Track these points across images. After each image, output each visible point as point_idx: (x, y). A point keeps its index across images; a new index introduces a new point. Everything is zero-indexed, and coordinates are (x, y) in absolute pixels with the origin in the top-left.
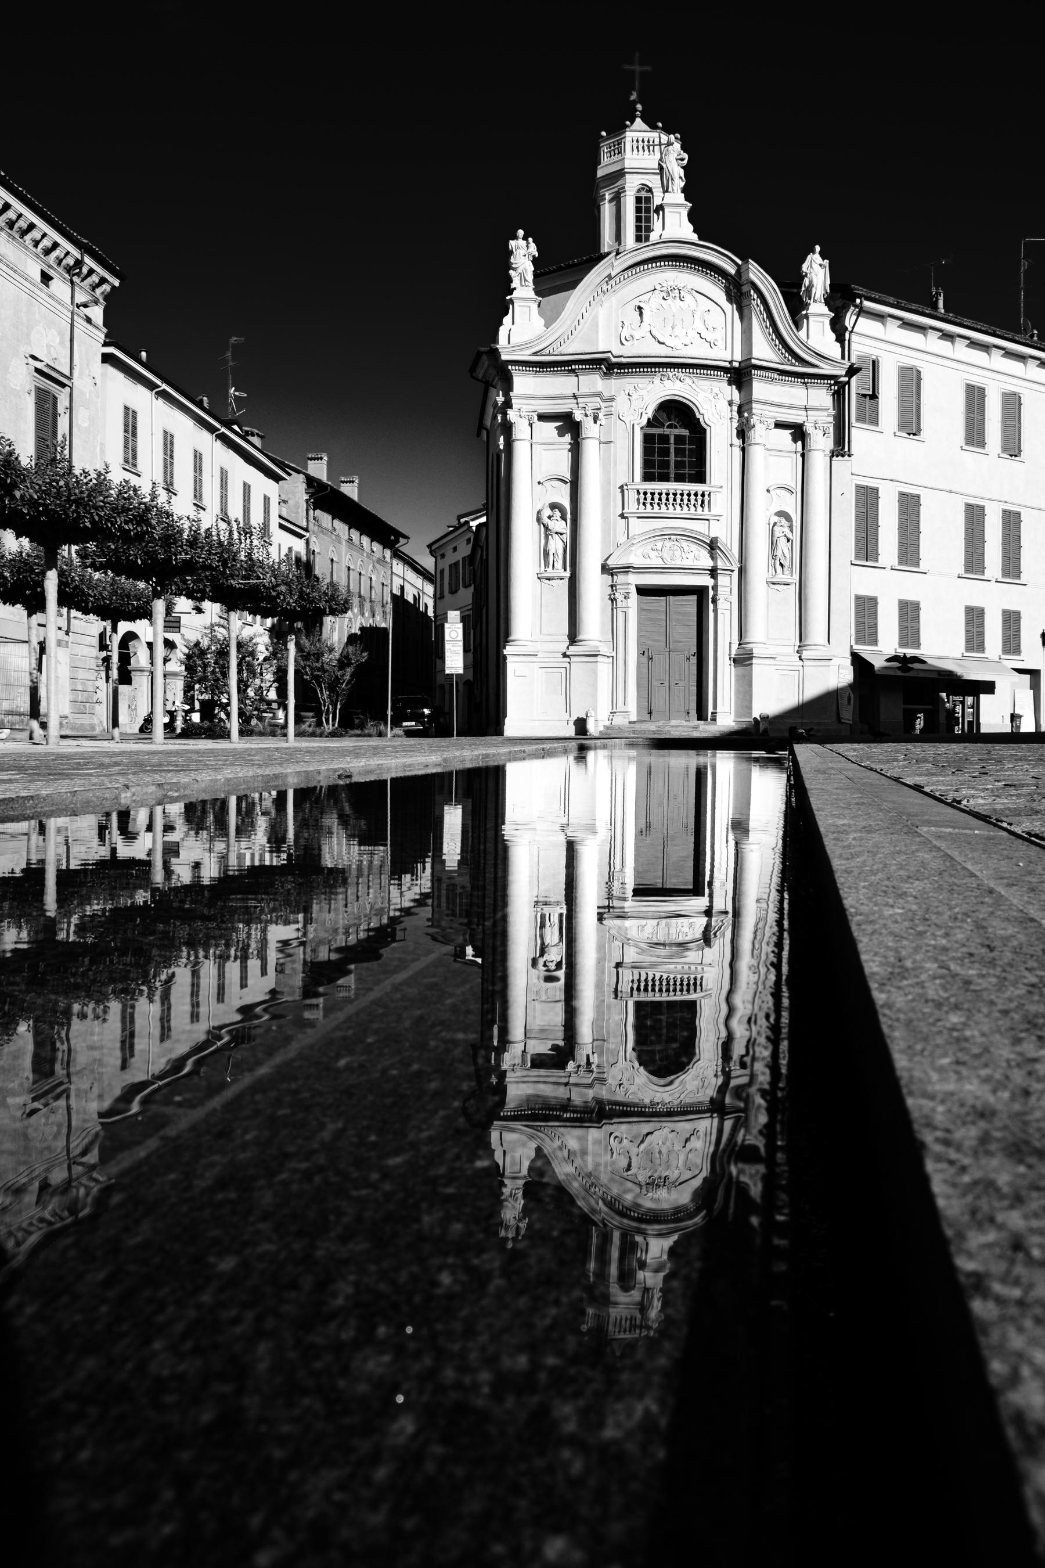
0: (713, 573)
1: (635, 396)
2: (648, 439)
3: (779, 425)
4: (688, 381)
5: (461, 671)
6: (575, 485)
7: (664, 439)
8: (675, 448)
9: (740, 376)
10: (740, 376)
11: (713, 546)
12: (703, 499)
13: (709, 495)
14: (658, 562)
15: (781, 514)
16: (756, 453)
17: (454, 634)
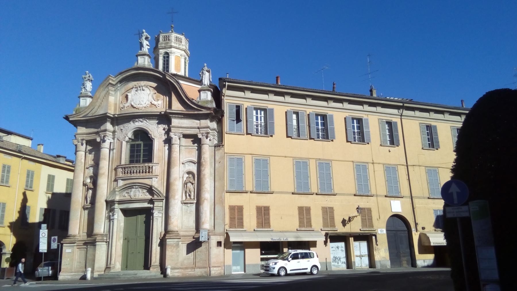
0: (151, 201)
1: (124, 129)
2: (132, 146)
3: (186, 136)
4: (145, 121)
5: (46, 251)
6: (199, 163)
7: (139, 145)
8: (142, 148)
9: (164, 118)
10: (164, 118)
11: (150, 190)
12: (150, 170)
13: (152, 168)
14: (127, 198)
15: (189, 173)
16: (176, 148)
17: (43, 235)
